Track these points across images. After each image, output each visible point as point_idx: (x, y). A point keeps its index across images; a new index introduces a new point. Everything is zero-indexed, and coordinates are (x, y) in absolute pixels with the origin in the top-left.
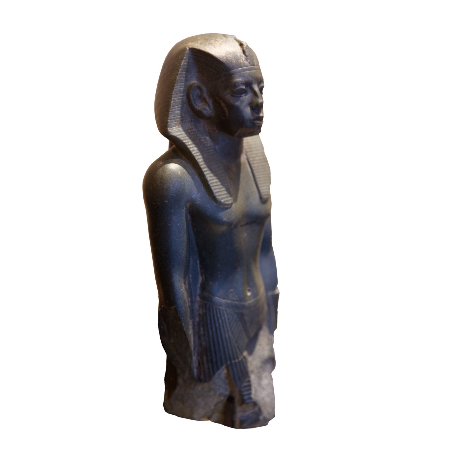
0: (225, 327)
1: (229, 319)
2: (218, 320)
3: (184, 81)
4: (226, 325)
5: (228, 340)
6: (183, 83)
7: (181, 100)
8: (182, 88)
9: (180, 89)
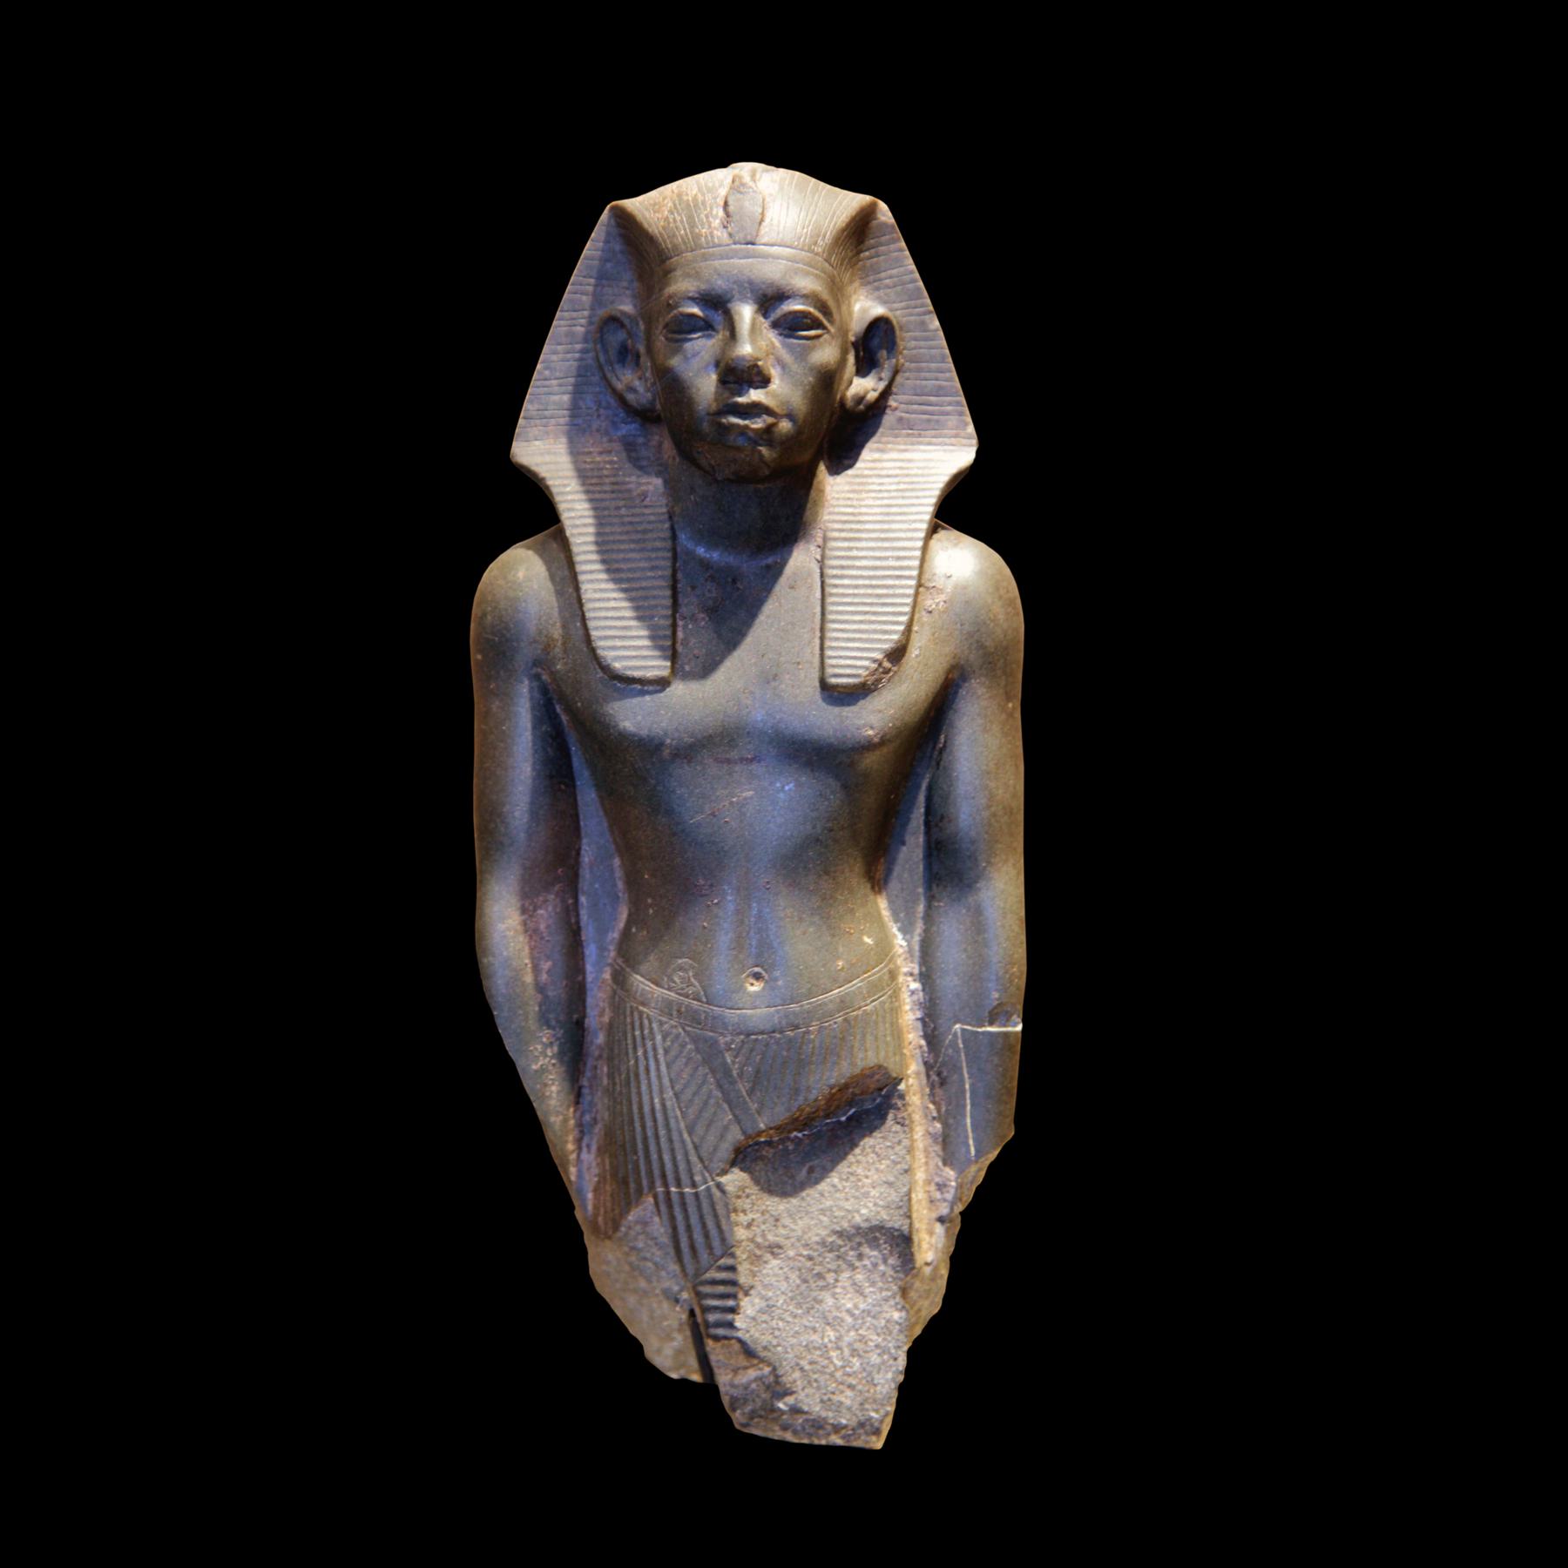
0: (653, 1073)
1: (666, 1051)
2: (635, 1048)
3: (588, 308)
4: (658, 1069)
5: (659, 1116)
6: (586, 313)
7: (575, 364)
8: (582, 326)
9: (574, 328)
